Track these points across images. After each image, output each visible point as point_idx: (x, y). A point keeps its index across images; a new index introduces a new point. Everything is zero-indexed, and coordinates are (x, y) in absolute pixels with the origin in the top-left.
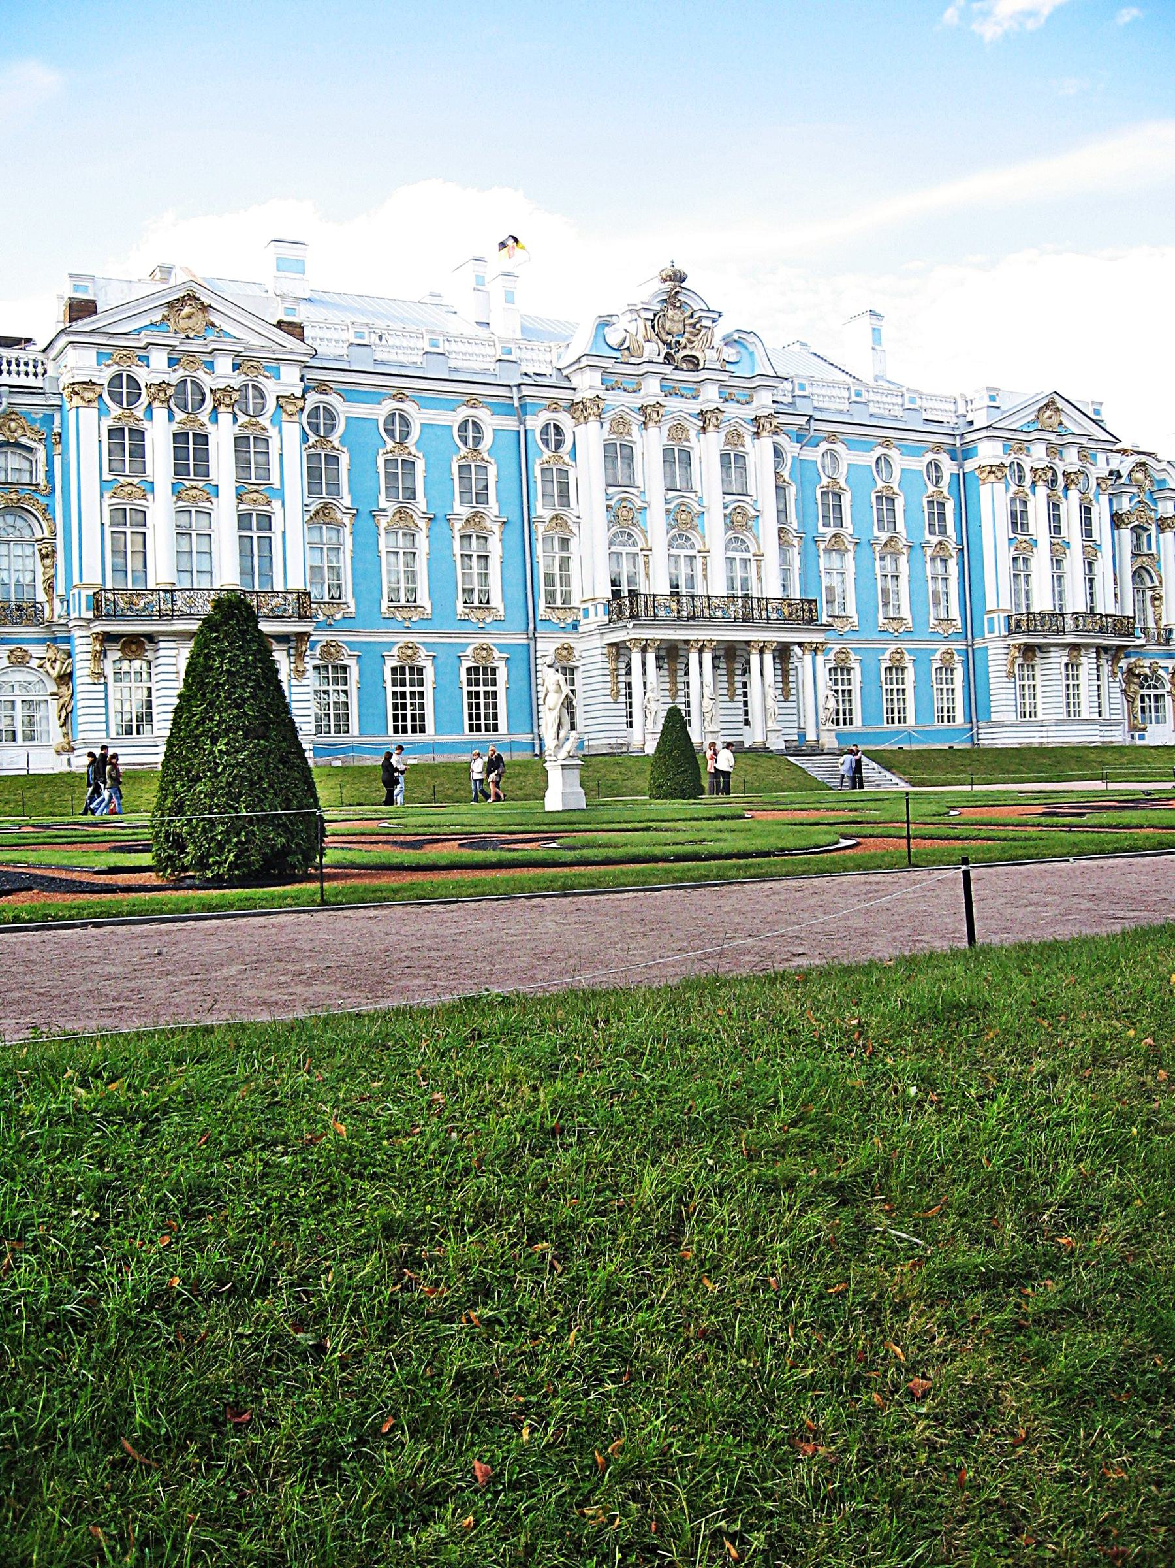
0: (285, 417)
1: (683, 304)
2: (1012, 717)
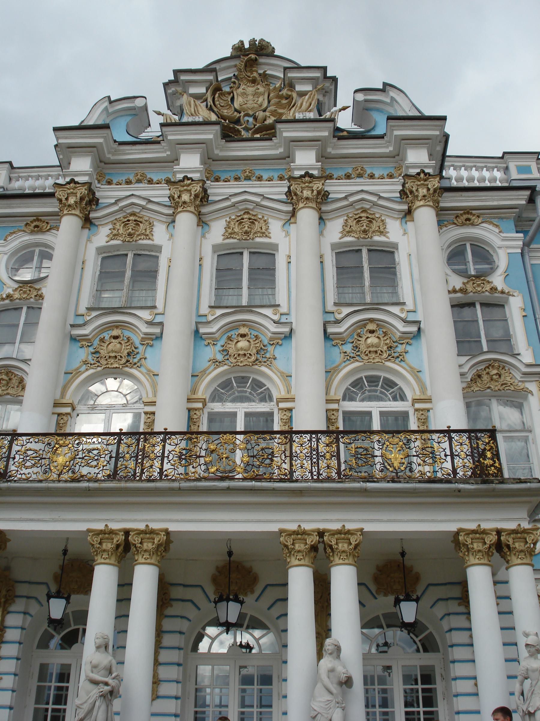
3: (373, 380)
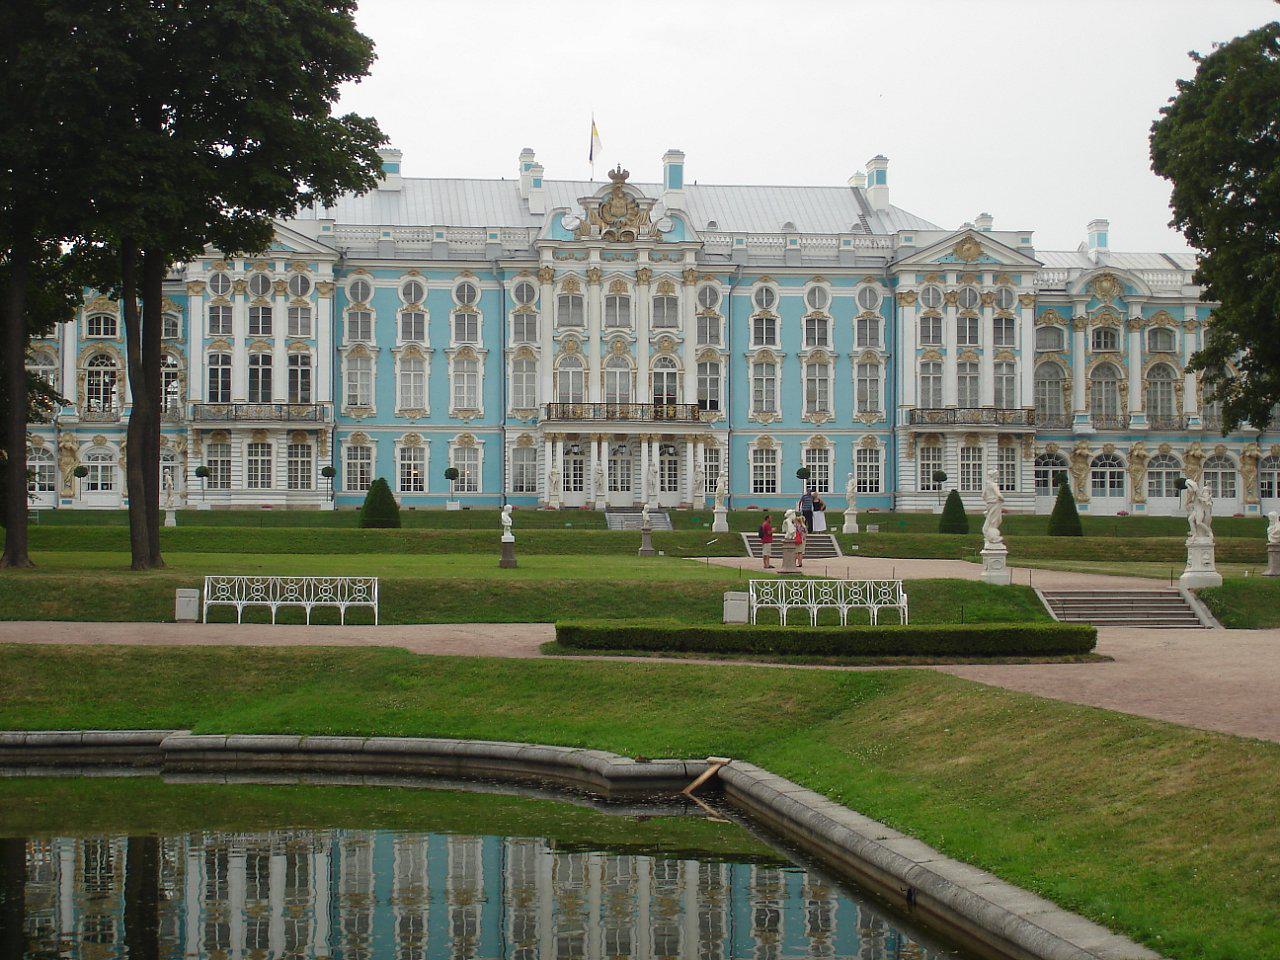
0: (320, 295)
1: (624, 194)
2: (913, 489)
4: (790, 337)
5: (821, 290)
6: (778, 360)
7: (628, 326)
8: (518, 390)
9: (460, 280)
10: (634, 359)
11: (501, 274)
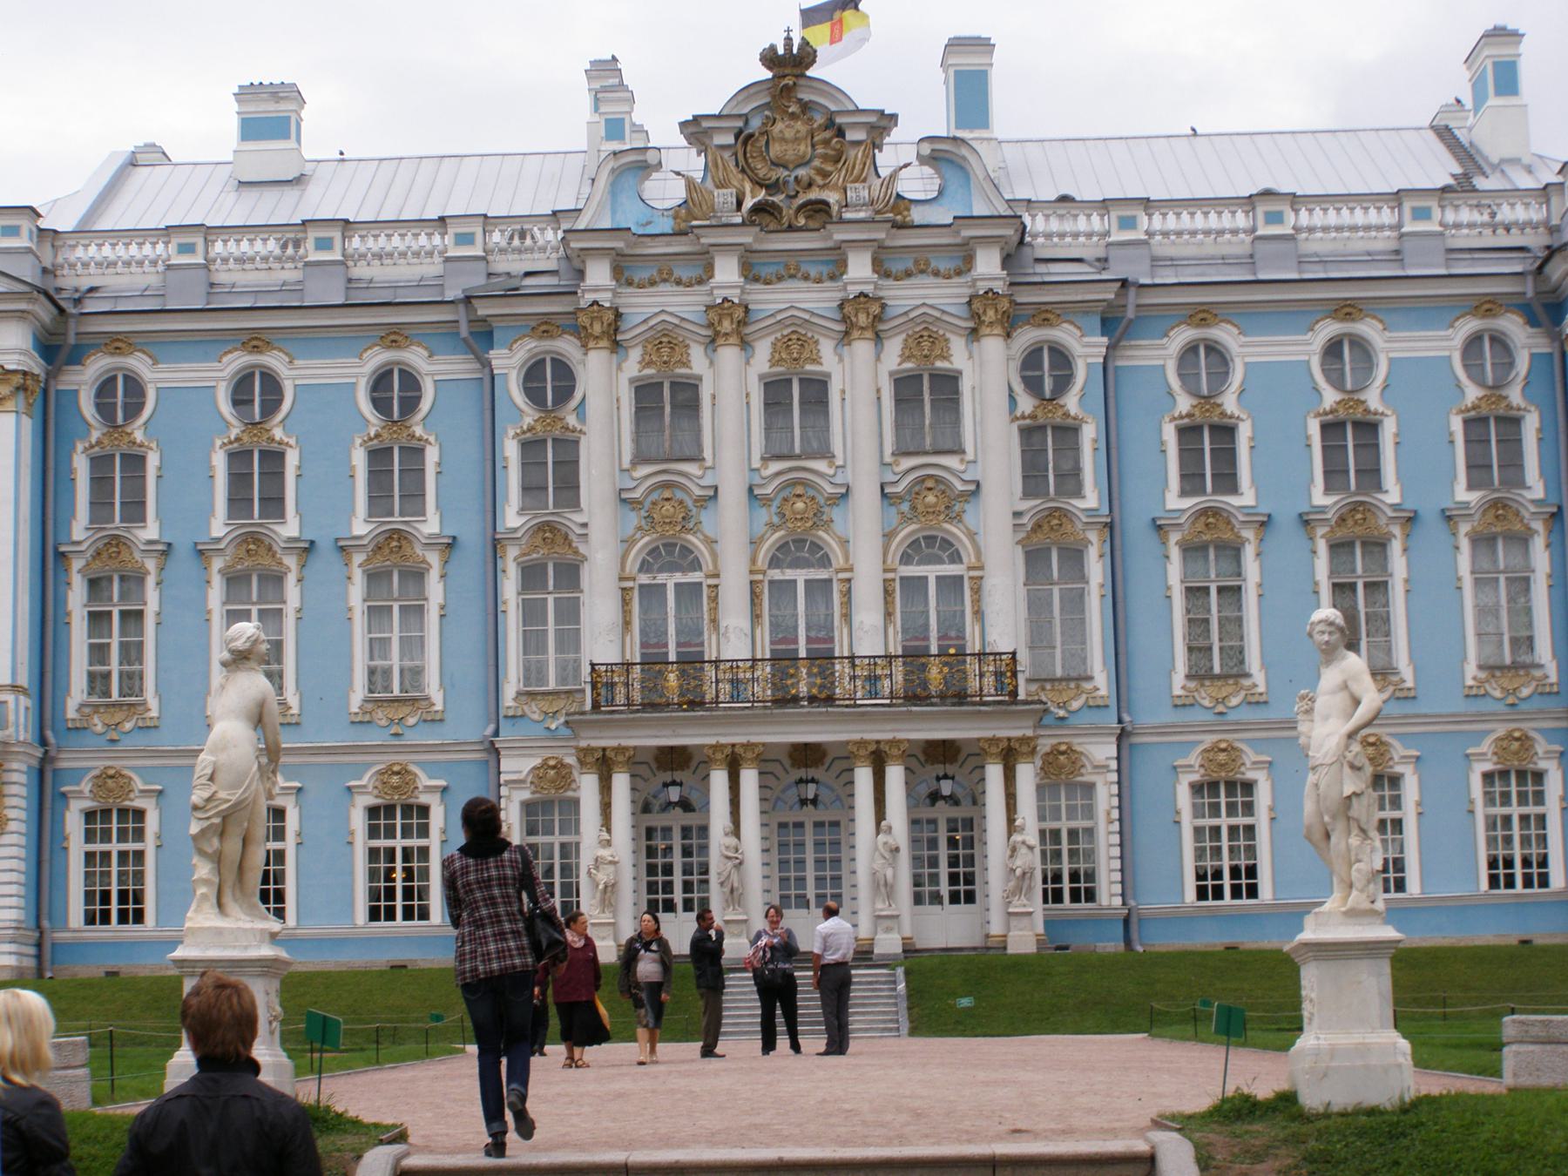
1: (806, 107)
3: (930, 539)
4: (1279, 471)
5: (1361, 346)
6: (1248, 534)
7: (826, 454)
8: (533, 642)
9: (378, 358)
10: (844, 543)
11: (482, 336)
